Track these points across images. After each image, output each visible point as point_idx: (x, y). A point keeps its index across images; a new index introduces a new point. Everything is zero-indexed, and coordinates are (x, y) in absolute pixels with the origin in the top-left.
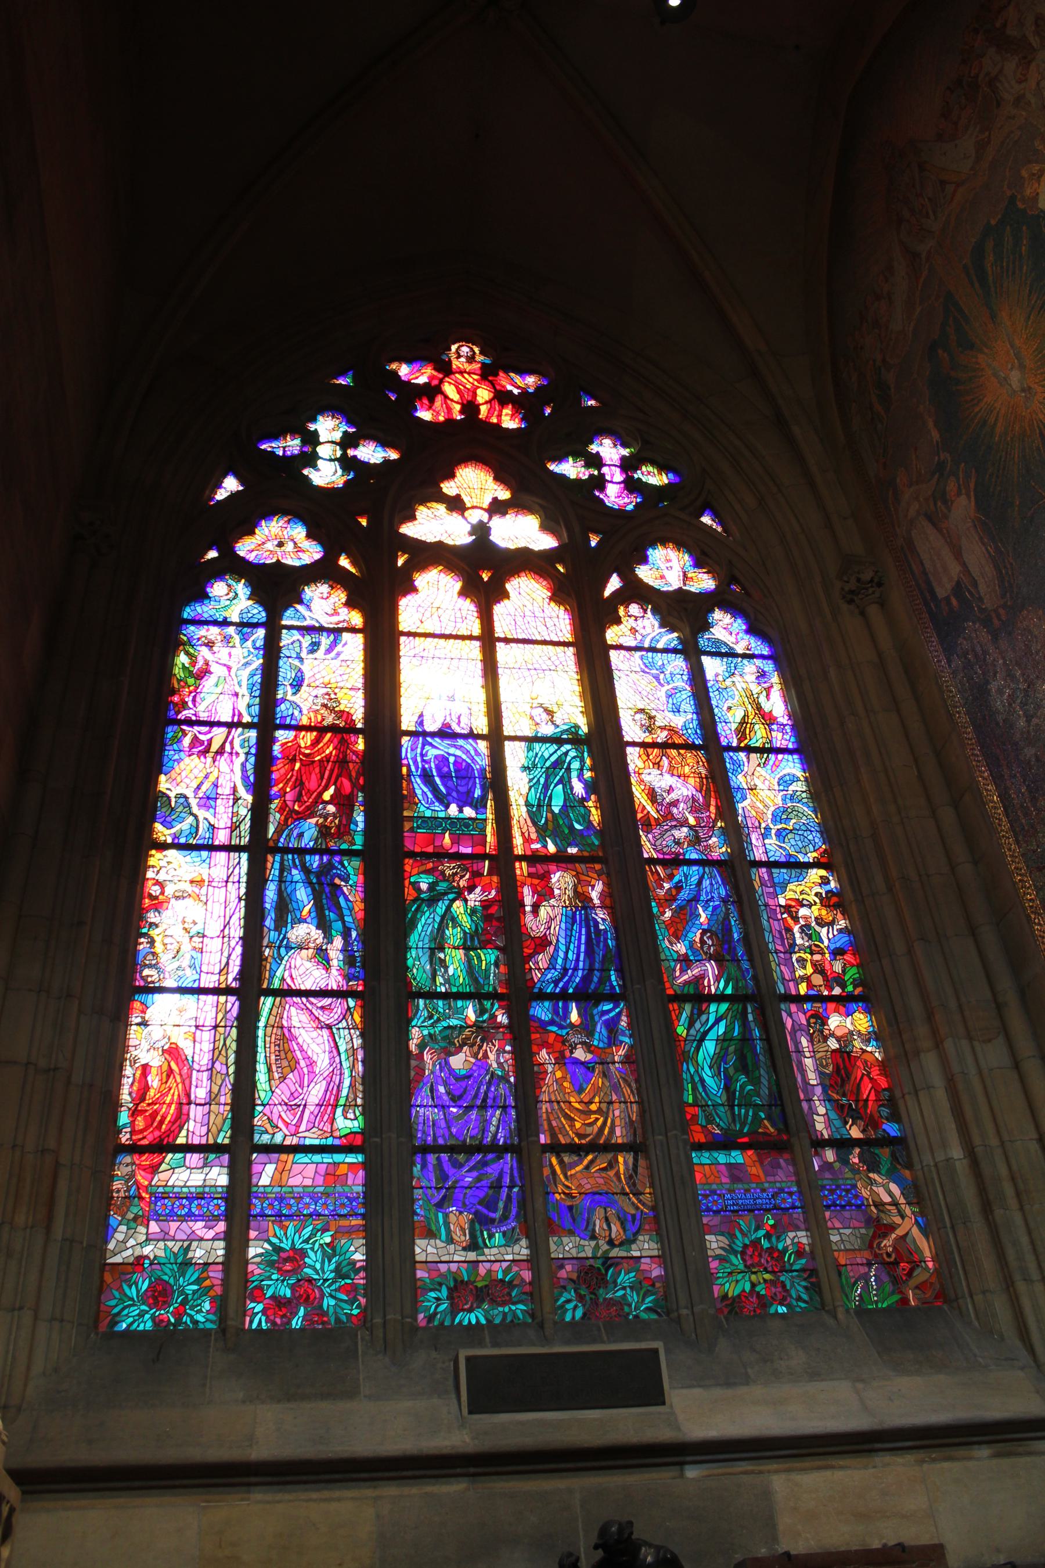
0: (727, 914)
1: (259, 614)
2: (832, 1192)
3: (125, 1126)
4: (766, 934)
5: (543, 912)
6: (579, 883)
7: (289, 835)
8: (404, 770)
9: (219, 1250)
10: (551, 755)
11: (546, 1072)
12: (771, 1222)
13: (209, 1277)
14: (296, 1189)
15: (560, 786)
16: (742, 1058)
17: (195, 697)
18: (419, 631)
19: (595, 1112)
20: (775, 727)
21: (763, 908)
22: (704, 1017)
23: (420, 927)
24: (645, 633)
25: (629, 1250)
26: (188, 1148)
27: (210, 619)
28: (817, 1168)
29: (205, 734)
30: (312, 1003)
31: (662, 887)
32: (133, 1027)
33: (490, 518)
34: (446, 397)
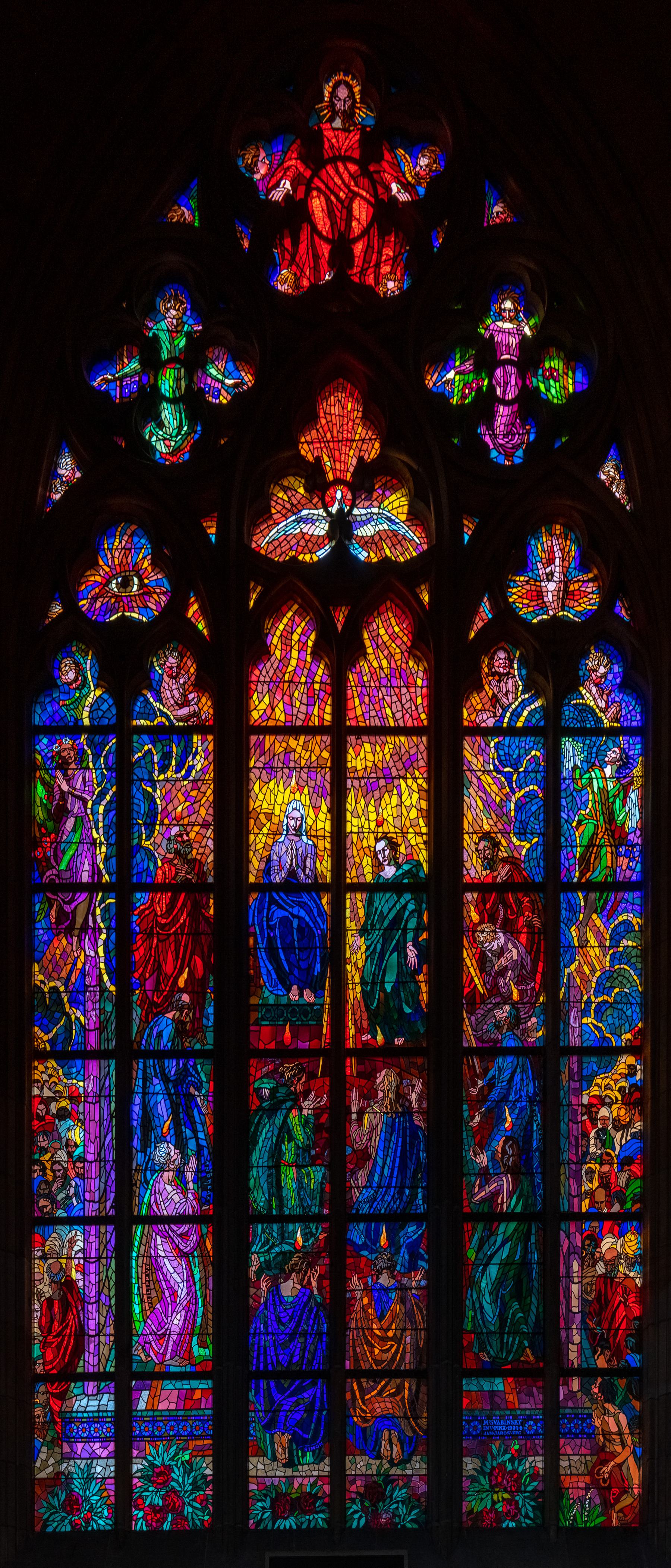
0: (531, 1117)
4: (562, 1141)
7: (149, 1036)
8: (251, 941)
10: (390, 910)
11: (355, 1298)
12: (517, 1447)
15: (396, 954)
16: (518, 1283)
17: (56, 849)
18: (271, 723)
19: (391, 1339)
20: (622, 850)
21: (566, 1108)
22: (493, 1239)
25: (404, 1469)
26: (86, 1377)
28: (562, 1397)
29: (69, 903)
30: (173, 1231)
31: (475, 1084)
32: (37, 1261)
34: (314, 229)
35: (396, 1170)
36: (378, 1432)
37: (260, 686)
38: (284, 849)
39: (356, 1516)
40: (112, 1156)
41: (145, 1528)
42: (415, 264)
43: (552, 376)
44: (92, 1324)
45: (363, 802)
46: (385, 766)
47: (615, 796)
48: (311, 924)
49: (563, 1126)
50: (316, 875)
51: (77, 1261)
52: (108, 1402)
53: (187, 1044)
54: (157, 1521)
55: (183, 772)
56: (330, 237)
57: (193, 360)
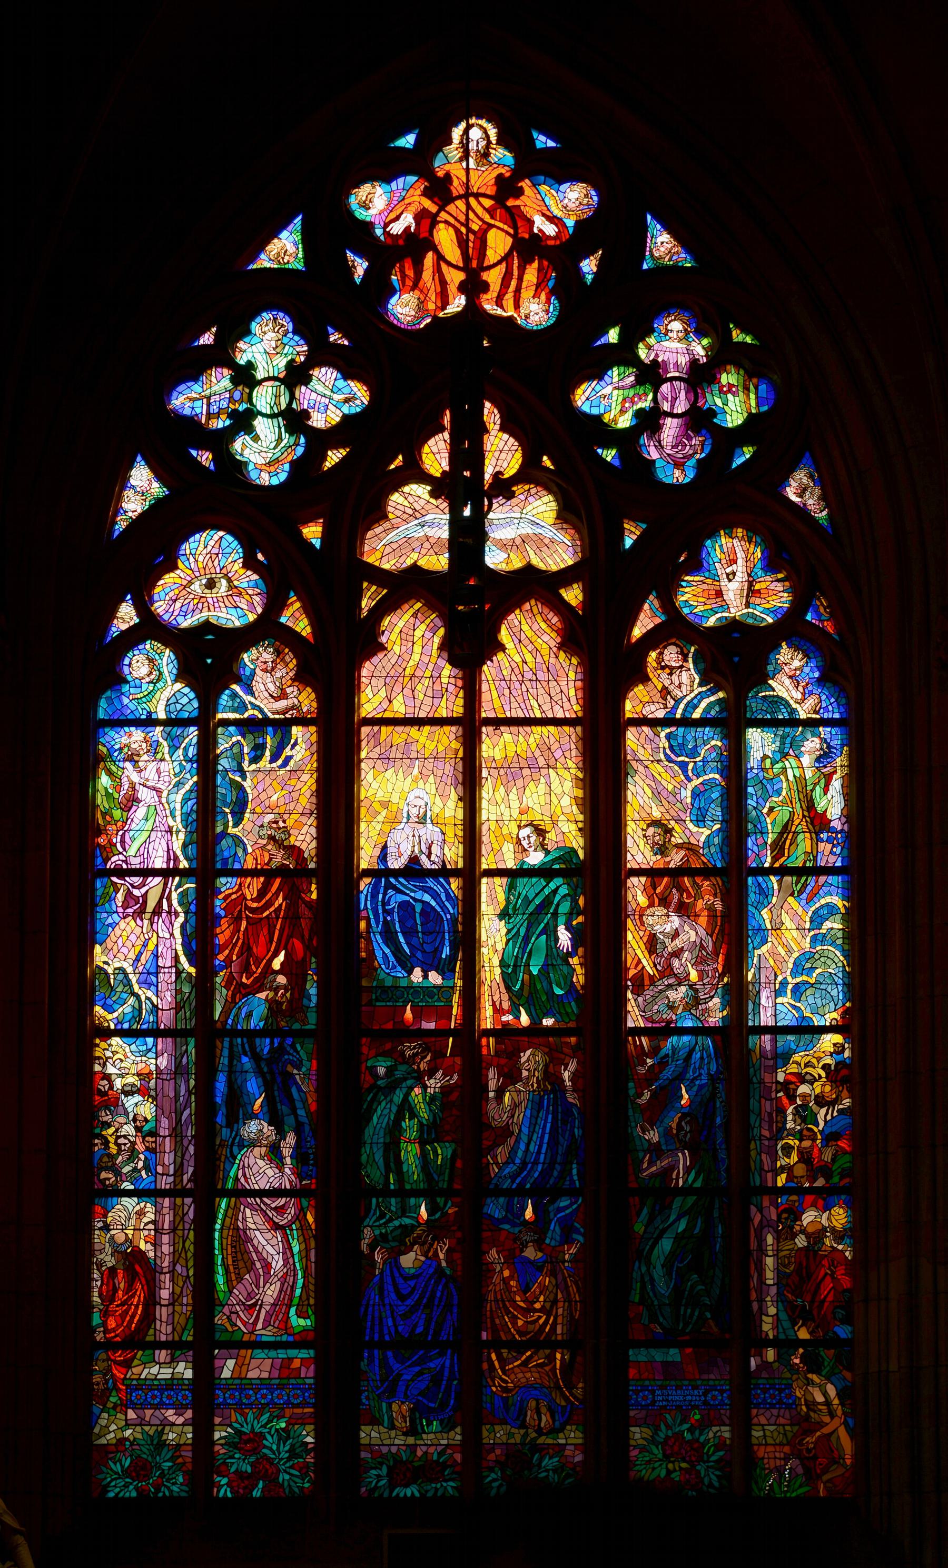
1: (188, 702)
2: (764, 1391)
3: (98, 1326)
4: (753, 1118)
7: (237, 1015)
8: (363, 925)
10: (537, 895)
12: (697, 1417)
13: (181, 1456)
17: (123, 836)
18: (388, 715)
20: (824, 836)
23: (375, 1119)
24: (680, 695)
27: (131, 717)
34: (440, 257)
35: (545, 1146)
39: (495, 1484)
41: (229, 1495)
42: (565, 287)
43: (729, 391)
44: (165, 1294)
45: (502, 790)
46: (530, 755)
47: (815, 784)
48: (438, 908)
50: (443, 861)
51: (146, 1233)
54: (244, 1488)
55: (279, 762)
56: (461, 264)
57: (296, 376)
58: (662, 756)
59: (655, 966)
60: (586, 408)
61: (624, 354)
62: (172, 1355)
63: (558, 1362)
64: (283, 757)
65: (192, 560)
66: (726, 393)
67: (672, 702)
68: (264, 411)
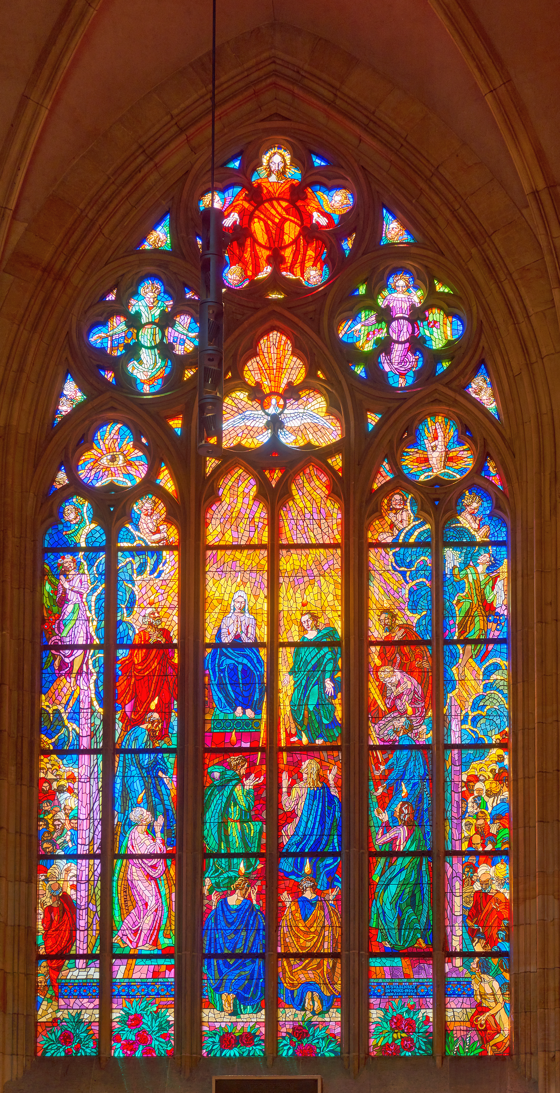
5: (294, 792)
6: (321, 768)
8: (207, 679)
9: (96, 1015)
10: (313, 659)
12: (412, 1003)
14: (137, 980)
16: (413, 896)
17: (59, 624)
18: (222, 543)
19: (313, 933)
21: (449, 783)
22: (393, 867)
28: (447, 970)
29: (69, 657)
30: (145, 863)
31: (378, 769)
32: (41, 883)
33: (284, 407)
35: (317, 824)
36: (303, 993)
37: (213, 521)
38: (232, 621)
39: (286, 1048)
40: (99, 816)
44: (82, 923)
45: (291, 591)
47: (486, 584)
49: (448, 795)
50: (255, 638)
52: (94, 973)
53: (157, 745)
55: (155, 574)
56: (268, 245)
57: (166, 321)
58: (390, 567)
59: (386, 704)
60: (345, 339)
61: (369, 302)
62: (87, 963)
63: (325, 967)
64: (158, 571)
65: (101, 443)
66: (432, 327)
67: (397, 532)
68: (146, 345)
